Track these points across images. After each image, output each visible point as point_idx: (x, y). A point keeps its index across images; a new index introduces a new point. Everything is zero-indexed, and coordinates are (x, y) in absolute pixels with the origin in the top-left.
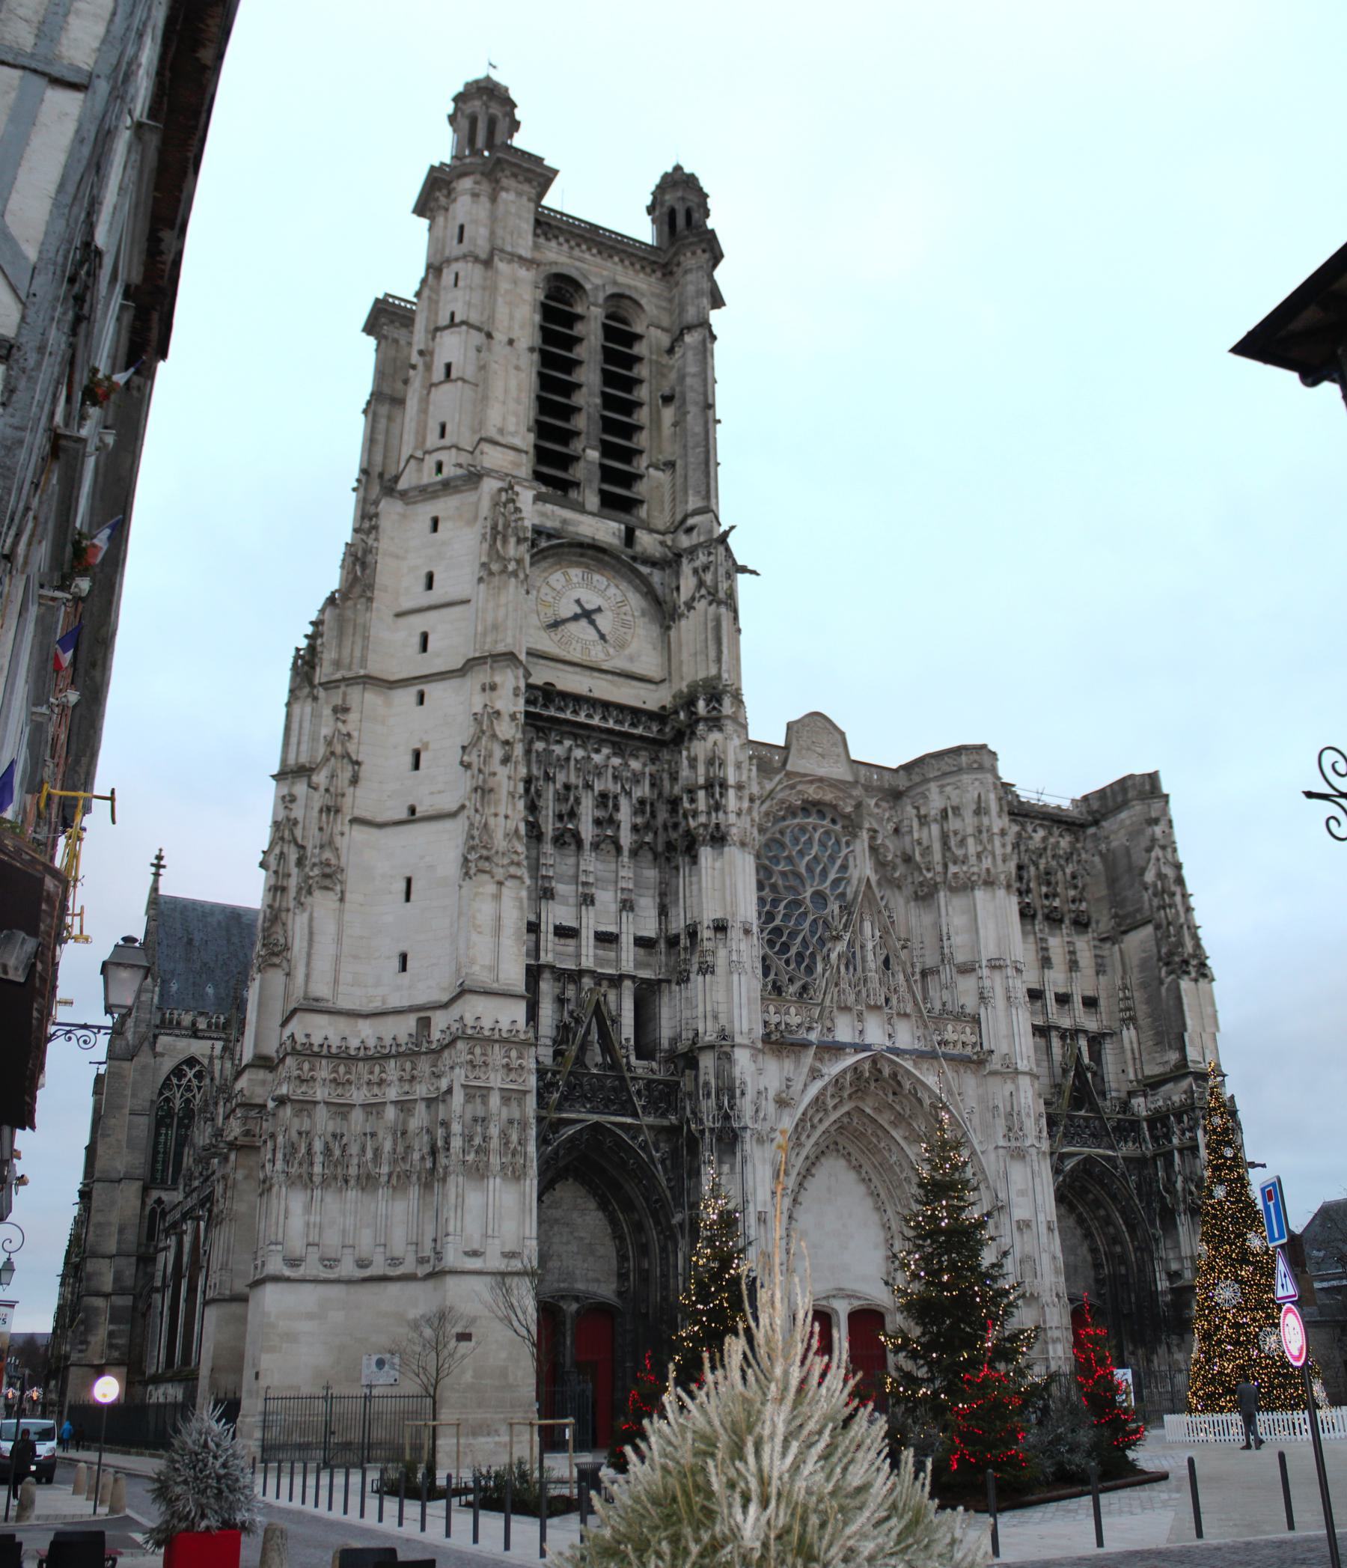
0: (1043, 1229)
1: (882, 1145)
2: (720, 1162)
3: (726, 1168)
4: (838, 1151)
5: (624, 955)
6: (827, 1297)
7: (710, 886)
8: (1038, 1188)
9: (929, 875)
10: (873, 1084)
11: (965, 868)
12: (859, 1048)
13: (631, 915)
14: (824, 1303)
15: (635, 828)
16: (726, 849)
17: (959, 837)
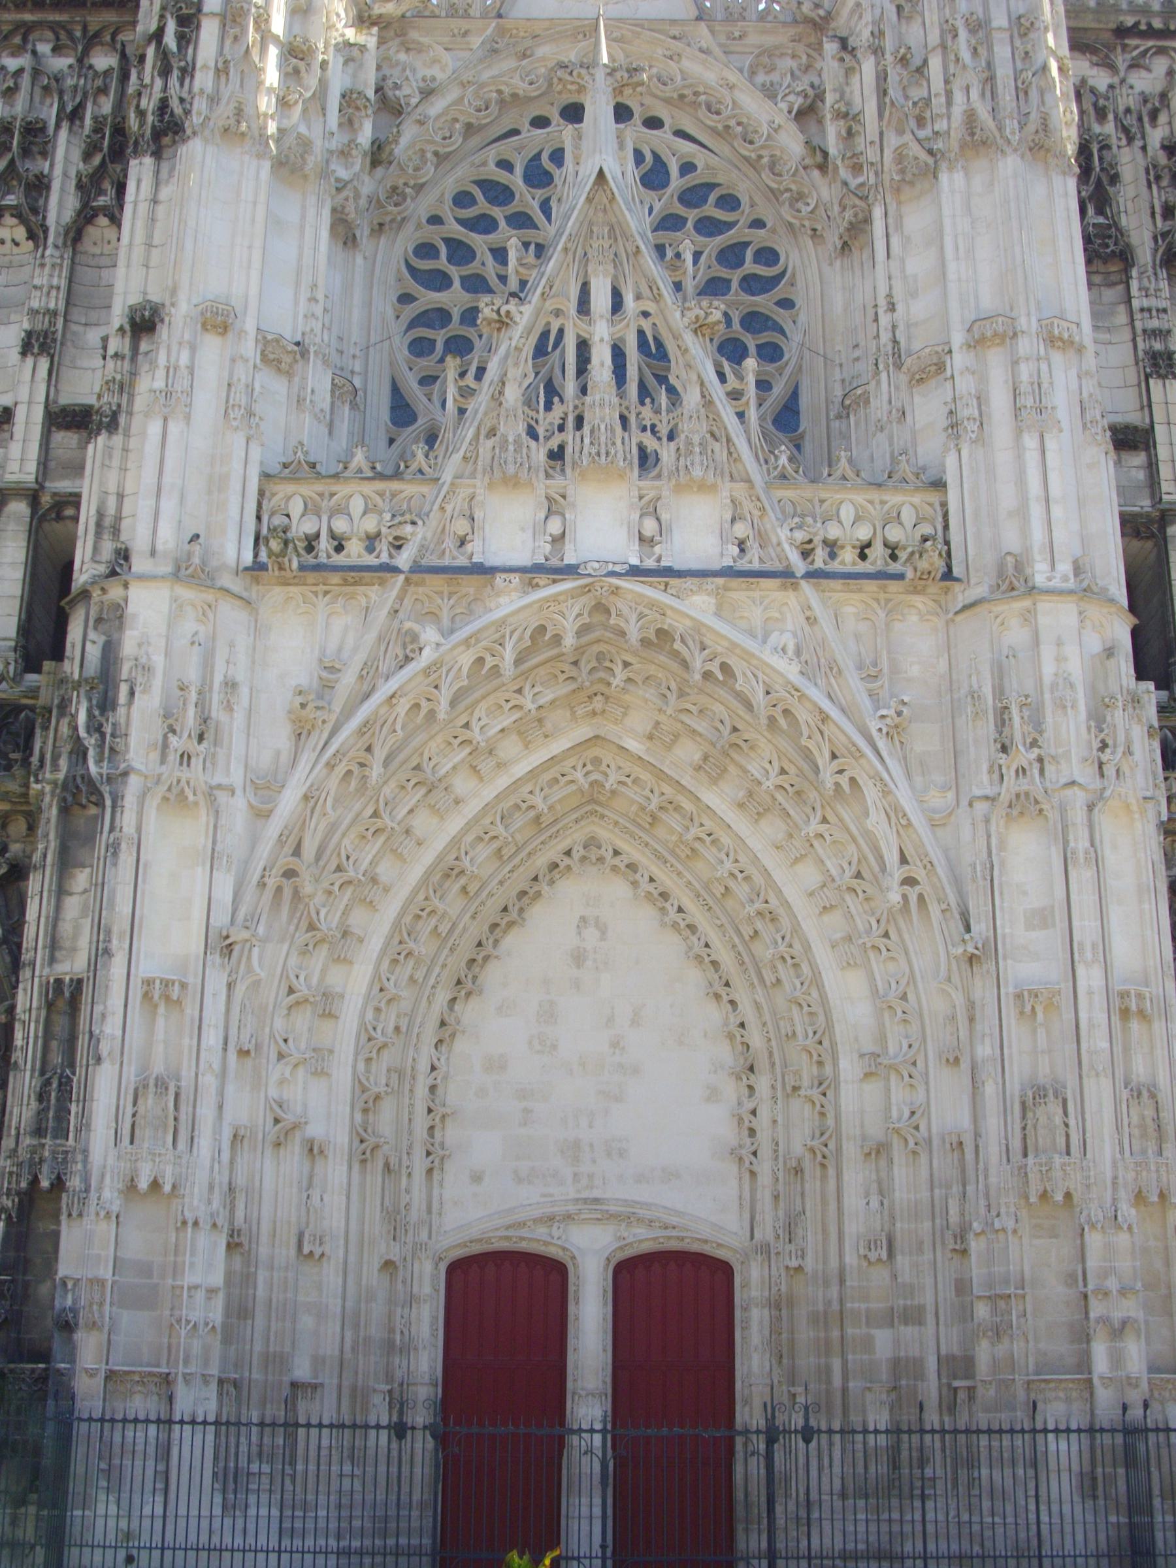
0: (1094, 1012)
1: (694, 831)
2: (66, 863)
3: (81, 879)
4: (601, 860)
5: (15, 449)
6: (550, 1219)
7: (140, 237)
8: (1085, 900)
9: (854, 183)
10: (620, 675)
11: (921, 134)
12: (533, 573)
13: (44, 364)
14: (541, 1231)
15: (80, 186)
16: (183, 150)
17: (917, 61)
